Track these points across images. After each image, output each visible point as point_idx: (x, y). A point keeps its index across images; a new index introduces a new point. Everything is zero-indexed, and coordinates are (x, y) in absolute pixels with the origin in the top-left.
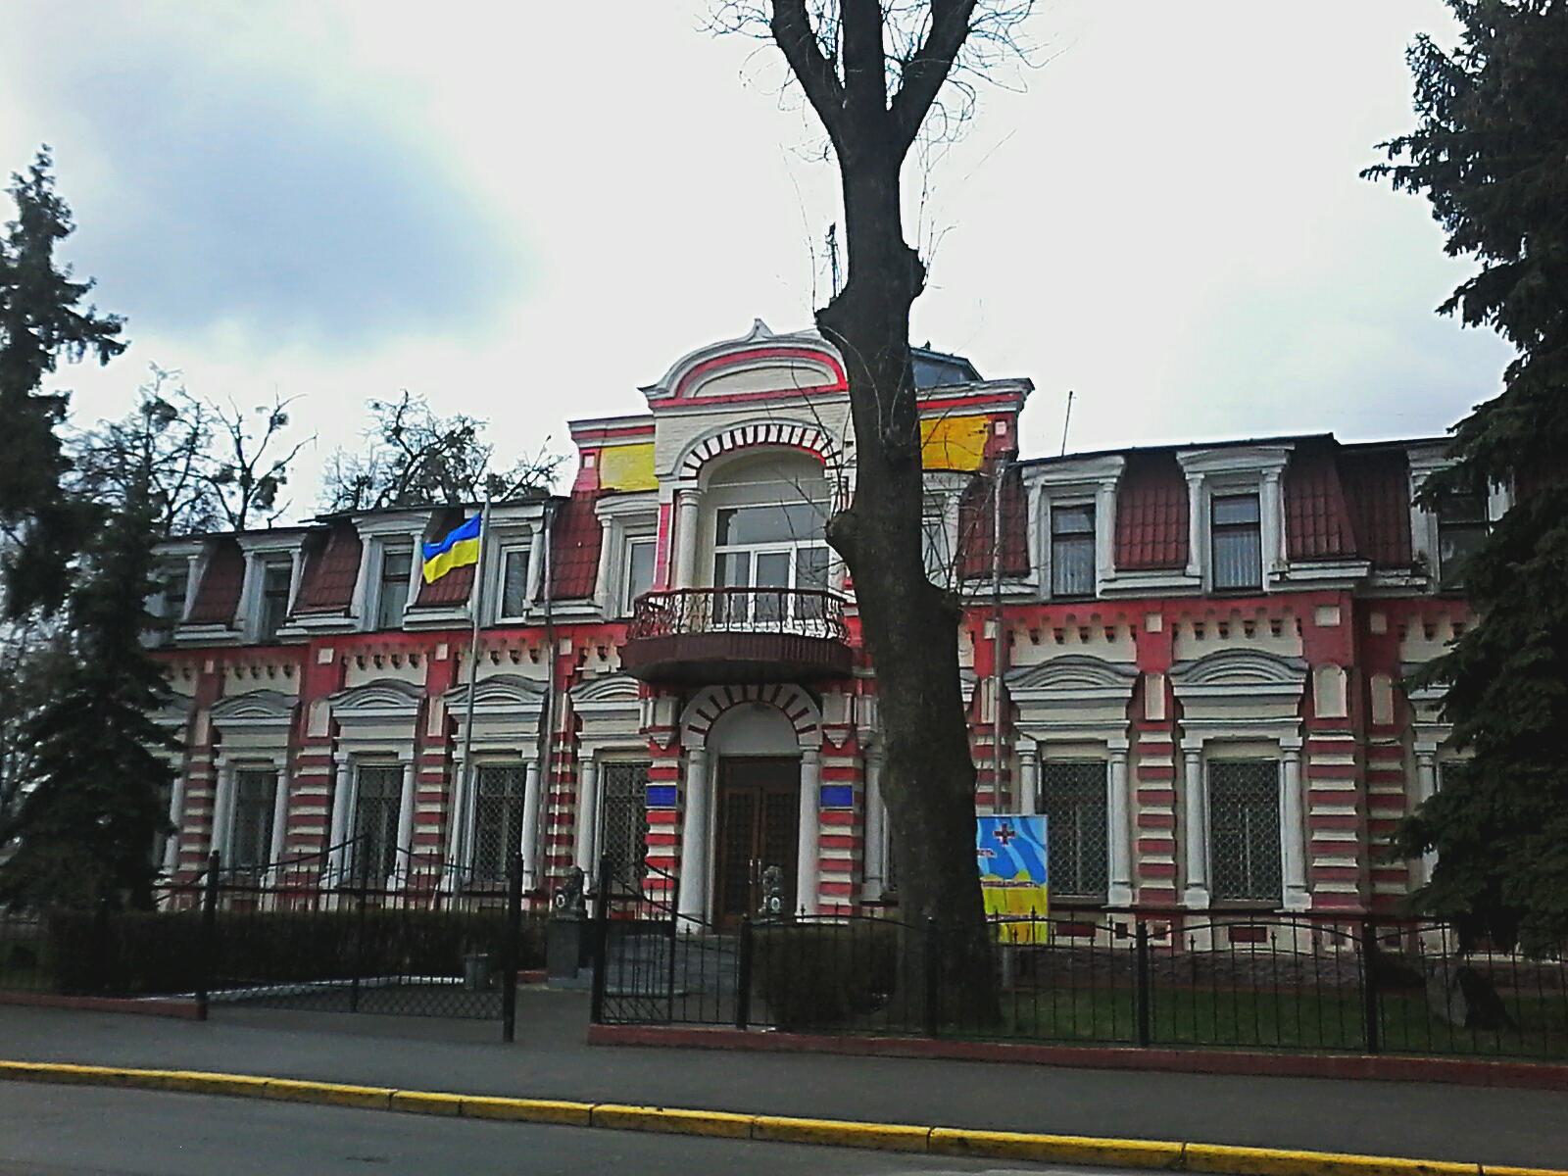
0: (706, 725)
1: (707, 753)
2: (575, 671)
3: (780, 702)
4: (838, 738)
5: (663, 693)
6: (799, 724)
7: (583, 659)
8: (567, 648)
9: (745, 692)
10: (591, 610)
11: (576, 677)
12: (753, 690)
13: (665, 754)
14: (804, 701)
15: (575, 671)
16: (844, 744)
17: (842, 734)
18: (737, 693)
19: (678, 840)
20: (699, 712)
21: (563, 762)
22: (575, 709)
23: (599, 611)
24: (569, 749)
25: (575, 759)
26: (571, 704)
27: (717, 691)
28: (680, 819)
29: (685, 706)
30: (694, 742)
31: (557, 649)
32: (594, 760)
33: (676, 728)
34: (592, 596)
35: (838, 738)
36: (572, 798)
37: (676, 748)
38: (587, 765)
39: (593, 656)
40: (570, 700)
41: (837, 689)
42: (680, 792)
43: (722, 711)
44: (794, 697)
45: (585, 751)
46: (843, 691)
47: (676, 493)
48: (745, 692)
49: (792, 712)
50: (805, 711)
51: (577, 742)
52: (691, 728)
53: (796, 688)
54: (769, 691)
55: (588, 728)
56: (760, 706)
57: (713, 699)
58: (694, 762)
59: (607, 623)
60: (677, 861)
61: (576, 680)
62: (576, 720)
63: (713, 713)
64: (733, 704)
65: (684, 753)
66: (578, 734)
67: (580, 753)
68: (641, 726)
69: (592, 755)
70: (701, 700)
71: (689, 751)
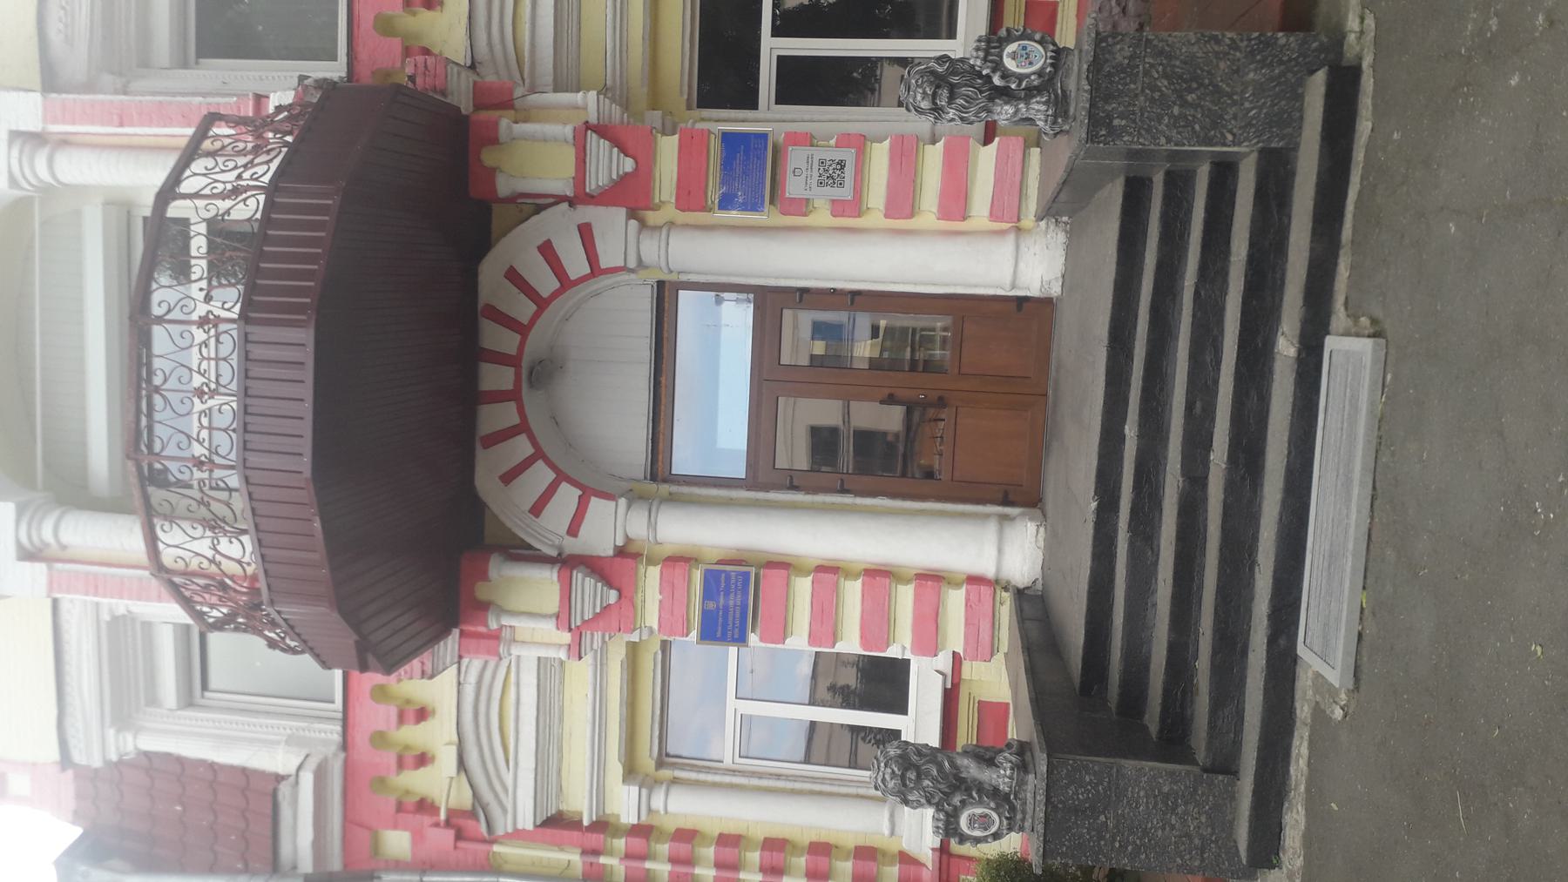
0: (568, 496)
1: (635, 497)
2: (448, 824)
3: (523, 309)
4: (606, 164)
5: (482, 591)
6: (576, 264)
7: (425, 806)
8: (397, 842)
9: (500, 397)
10: (307, 779)
11: (462, 822)
12: (495, 377)
13: (627, 593)
14: (517, 248)
15: (448, 824)
16: (624, 151)
17: (599, 148)
18: (495, 417)
19: (829, 572)
20: (537, 509)
21: (643, 857)
22: (530, 827)
23: (312, 764)
24: (620, 844)
25: (642, 831)
26: (518, 835)
27: (487, 468)
28: (783, 565)
29: (530, 547)
30: (607, 526)
31: (398, 866)
32: (649, 784)
33: (567, 563)
34: (279, 778)
35: (606, 164)
36: (729, 841)
37: (615, 568)
38: (658, 802)
39: (419, 782)
40: (508, 836)
41: (489, 157)
42: (720, 562)
43: (539, 454)
44: (513, 276)
45: (625, 804)
46: (494, 141)
47: (29, 554)
48: (500, 397)
49: (546, 283)
50: (547, 251)
51: (602, 825)
52: (573, 530)
53: (490, 272)
54: (496, 338)
55: (579, 802)
56: (543, 372)
57: (509, 477)
58: (652, 525)
59: (345, 745)
60: (879, 576)
61: (469, 824)
62: (556, 823)
63: (541, 476)
64: (523, 428)
65: (626, 552)
66: (586, 823)
67: (629, 817)
68: (563, 655)
69: (634, 789)
70: (509, 505)
71: (628, 540)
